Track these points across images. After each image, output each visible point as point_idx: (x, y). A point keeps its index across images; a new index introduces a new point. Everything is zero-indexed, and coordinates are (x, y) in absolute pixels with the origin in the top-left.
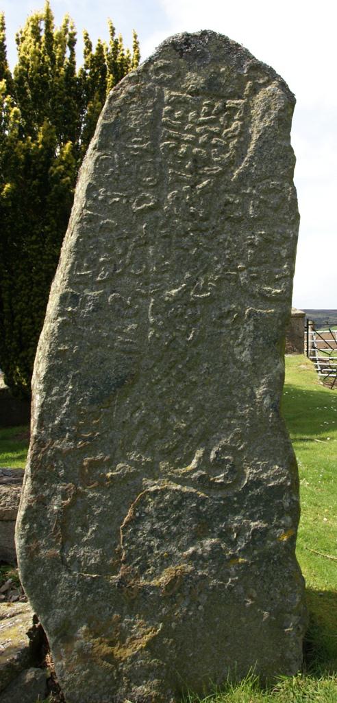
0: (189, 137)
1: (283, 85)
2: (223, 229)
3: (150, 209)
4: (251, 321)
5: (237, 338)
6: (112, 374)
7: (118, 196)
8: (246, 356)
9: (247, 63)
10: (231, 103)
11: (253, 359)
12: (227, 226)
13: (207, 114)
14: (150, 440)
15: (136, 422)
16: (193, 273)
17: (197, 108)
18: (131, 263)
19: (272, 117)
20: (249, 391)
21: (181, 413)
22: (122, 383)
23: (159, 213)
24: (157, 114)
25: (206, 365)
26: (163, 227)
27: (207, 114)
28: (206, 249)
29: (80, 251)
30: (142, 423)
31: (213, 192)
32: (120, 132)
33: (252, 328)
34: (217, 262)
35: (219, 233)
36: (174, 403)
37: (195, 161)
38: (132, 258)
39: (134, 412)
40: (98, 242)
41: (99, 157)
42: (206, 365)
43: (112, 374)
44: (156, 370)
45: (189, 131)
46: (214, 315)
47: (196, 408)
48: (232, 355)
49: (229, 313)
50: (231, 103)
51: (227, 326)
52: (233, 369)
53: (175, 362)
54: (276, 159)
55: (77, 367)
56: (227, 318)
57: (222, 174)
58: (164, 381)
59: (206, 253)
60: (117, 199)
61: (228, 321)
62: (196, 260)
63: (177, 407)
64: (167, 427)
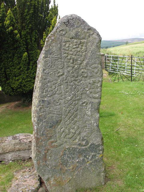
0: (71, 53)
1: (98, 35)
2: (82, 79)
3: (61, 75)
4: (91, 104)
5: (87, 109)
6: (55, 120)
7: (52, 72)
8: (89, 113)
9: (86, 28)
10: (83, 41)
11: (91, 114)
12: (83, 79)
13: (76, 45)
14: (66, 135)
15: (62, 131)
16: (73, 178)
17: (72, 43)
18: (57, 91)
19: (95, 45)
20: (90, 122)
21: (73, 128)
22: (58, 122)
23: (64, 76)
24: (61, 45)
25: (79, 116)
26: (65, 80)
27: (76, 45)
28: (78, 85)
29: (42, 89)
30: (63, 131)
31: (79, 69)
32: (51, 52)
33: (91, 106)
34: (81, 89)
35: (81, 81)
36: (71, 126)
37: (73, 60)
38: (57, 89)
39: (61, 129)
40: (47, 85)
41: (45, 60)
42: (79, 116)
43: (55, 120)
44: (66, 118)
45: (71, 51)
46: (81, 103)
47: (77, 127)
48: (86, 113)
49: (84, 103)
50: (83, 41)
51: (84, 106)
52: (86, 117)
53: (71, 116)
54: (96, 58)
55: (45, 119)
56: (84, 104)
57: (81, 64)
58: (69, 121)
59: (77, 87)
60: (52, 73)
61: (84, 105)
62: (75, 89)
63: (72, 127)
64: (69, 132)
